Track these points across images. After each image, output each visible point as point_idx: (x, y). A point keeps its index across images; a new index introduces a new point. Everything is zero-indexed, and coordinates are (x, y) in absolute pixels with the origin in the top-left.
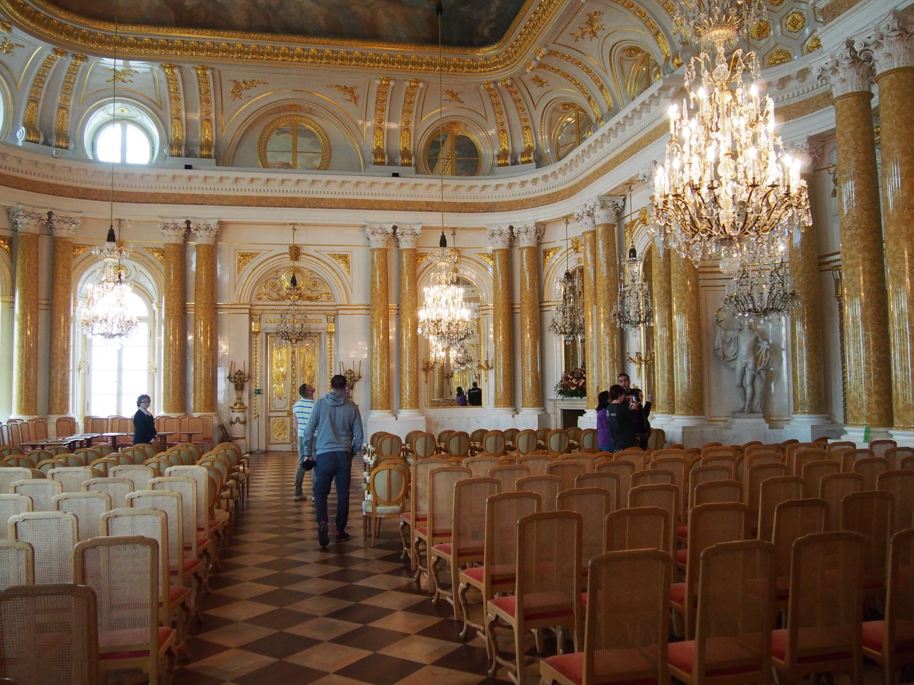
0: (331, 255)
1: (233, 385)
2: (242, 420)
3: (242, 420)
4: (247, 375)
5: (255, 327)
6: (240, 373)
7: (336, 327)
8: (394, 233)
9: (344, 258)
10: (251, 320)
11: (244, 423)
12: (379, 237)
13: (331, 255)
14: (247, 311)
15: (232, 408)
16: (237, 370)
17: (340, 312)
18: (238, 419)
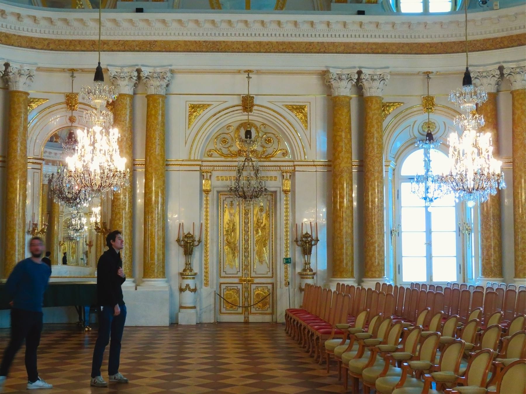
0: (287, 106)
1: (182, 250)
2: (192, 287)
3: (192, 287)
4: (197, 239)
5: (206, 185)
6: (189, 236)
7: (293, 185)
8: (359, 79)
9: (299, 109)
10: (202, 177)
11: (195, 290)
12: (344, 83)
13: (287, 106)
14: (198, 168)
15: (181, 274)
16: (186, 232)
17: (297, 168)
18: (187, 285)
